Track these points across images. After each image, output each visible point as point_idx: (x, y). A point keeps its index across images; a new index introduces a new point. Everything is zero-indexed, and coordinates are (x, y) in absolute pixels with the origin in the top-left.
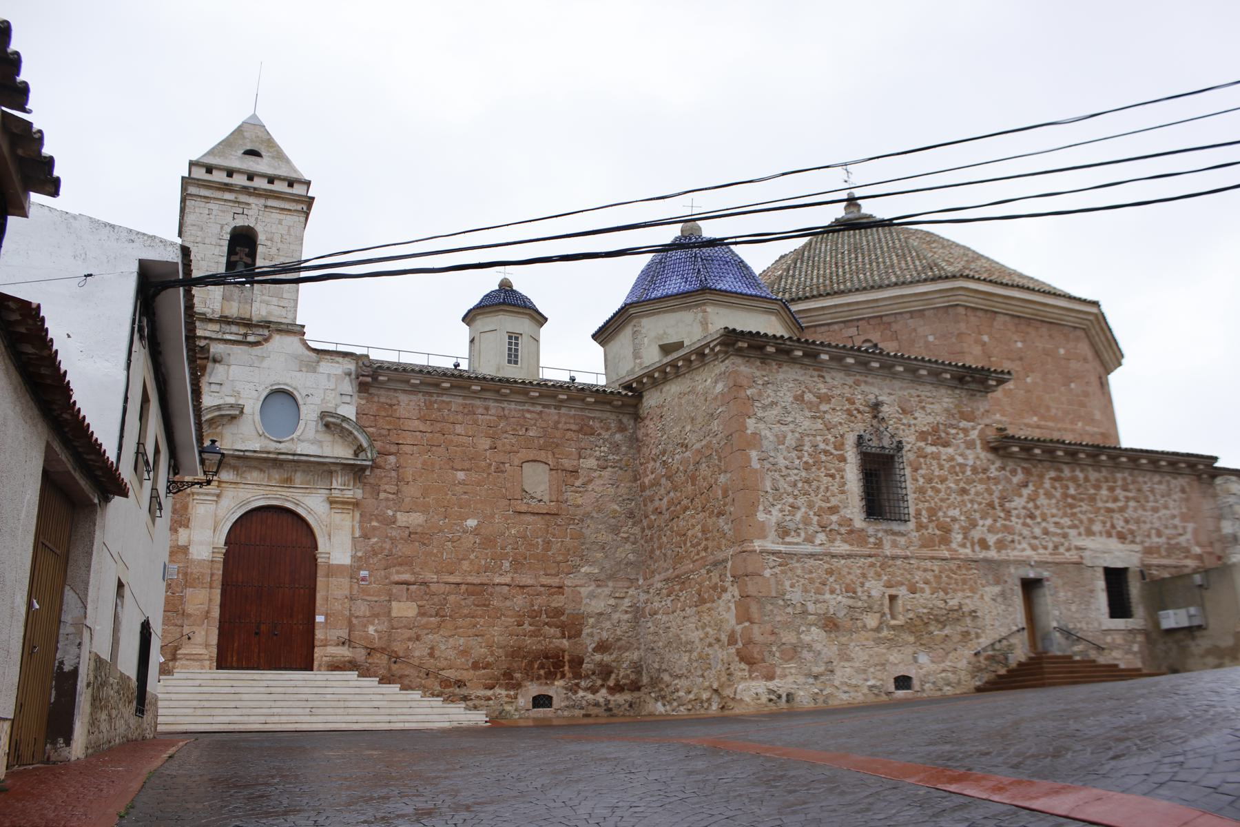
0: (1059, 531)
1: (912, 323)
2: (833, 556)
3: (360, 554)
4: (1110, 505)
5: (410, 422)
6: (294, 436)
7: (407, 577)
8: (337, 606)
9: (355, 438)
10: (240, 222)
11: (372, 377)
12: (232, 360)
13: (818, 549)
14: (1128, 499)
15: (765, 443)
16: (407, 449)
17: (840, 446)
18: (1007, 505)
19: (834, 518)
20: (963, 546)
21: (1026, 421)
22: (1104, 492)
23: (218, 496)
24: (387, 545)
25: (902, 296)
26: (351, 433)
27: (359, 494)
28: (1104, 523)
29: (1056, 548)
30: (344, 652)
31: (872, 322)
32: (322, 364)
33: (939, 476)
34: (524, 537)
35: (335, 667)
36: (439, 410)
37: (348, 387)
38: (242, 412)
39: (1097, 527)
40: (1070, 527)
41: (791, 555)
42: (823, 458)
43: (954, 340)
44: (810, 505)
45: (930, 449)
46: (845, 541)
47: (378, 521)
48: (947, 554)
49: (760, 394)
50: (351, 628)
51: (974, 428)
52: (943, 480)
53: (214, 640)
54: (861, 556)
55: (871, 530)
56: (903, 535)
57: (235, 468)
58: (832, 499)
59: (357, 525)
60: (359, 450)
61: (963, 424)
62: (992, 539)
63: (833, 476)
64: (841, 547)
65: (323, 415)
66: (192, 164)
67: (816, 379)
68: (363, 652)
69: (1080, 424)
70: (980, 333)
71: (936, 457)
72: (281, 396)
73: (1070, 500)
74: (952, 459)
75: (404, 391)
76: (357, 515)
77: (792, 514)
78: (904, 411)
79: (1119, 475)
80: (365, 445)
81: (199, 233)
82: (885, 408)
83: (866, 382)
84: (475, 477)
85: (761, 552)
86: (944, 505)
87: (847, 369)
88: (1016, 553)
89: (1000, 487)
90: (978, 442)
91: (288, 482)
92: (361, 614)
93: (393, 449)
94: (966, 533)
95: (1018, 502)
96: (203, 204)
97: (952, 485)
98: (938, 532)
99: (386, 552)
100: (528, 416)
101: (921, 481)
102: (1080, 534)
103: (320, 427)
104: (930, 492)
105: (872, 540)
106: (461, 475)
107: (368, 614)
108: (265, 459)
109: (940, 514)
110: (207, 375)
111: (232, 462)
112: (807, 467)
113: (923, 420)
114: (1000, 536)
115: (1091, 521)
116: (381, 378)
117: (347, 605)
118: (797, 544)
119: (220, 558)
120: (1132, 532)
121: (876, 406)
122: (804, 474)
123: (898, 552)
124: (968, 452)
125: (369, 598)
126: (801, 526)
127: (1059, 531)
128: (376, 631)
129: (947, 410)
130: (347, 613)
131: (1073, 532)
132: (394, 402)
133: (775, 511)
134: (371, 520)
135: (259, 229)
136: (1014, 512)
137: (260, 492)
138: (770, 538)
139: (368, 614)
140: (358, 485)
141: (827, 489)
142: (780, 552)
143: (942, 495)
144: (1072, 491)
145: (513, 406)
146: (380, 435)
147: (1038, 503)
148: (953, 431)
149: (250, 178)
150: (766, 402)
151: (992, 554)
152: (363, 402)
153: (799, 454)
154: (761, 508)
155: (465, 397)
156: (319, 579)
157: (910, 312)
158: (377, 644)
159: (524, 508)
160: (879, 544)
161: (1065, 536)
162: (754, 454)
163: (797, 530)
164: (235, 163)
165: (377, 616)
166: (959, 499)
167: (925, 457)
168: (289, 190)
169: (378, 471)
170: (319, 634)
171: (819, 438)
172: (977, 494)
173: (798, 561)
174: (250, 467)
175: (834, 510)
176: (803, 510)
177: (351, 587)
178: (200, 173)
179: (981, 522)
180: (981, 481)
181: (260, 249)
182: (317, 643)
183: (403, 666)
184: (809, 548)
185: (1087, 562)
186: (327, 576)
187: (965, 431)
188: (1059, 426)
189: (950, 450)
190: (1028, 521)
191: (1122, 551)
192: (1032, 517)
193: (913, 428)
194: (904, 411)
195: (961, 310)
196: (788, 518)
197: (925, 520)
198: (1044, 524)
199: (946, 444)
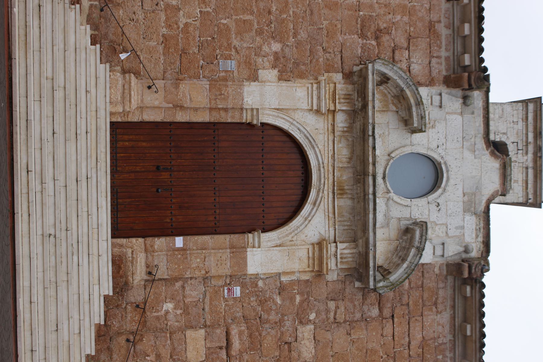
3: (260, 283)
5: (418, 328)
6: (392, 195)
7: (236, 345)
8: (195, 262)
9: (398, 266)
11: (467, 276)
12: (468, 117)
16: (388, 329)
23: (318, 112)
24: (273, 317)
26: (404, 260)
27: (332, 276)
30: (138, 274)
32: (474, 217)
35: (119, 265)
37: (453, 250)
38: (414, 131)
47: (302, 302)
50: (170, 281)
53: (149, 117)
57: (350, 129)
59: (294, 278)
60: (385, 272)
65: (423, 226)
68: (140, 299)
72: (436, 175)
75: (453, 318)
76: (306, 277)
80: (393, 278)
81: (497, 116)
91: (339, 191)
92: (188, 292)
93: (387, 312)
96: (521, 116)
99: (265, 316)
103: (404, 223)
107: (187, 300)
108: (364, 162)
110: (448, 90)
111: (358, 125)
116: (468, 288)
117: (197, 274)
119: (246, 118)
125: (207, 300)
128: (167, 312)
130: (188, 275)
132: (440, 307)
134: (301, 294)
137: (327, 160)
139: (187, 300)
140: (342, 274)
146: (401, 295)
152: (437, 270)
156: (228, 237)
158: (151, 315)
165: (186, 311)
169: (360, 296)
170: (159, 242)
174: (353, 146)
177: (220, 277)
182: (149, 240)
183: (123, 351)
186: (232, 247)
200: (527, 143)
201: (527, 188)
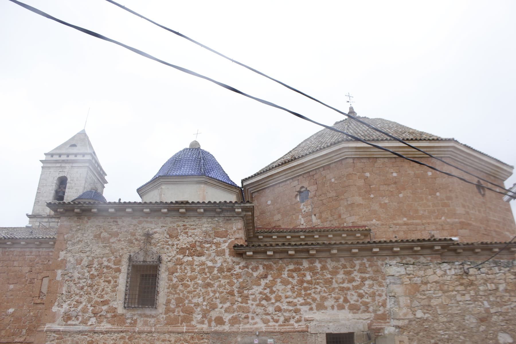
0: (291, 308)
1: (323, 173)
2: (95, 333)
4: (345, 285)
10: (61, 175)
13: (87, 328)
14: (363, 279)
15: (68, 265)
17: (118, 262)
18: (246, 292)
19: (105, 308)
20: (202, 323)
21: (395, 222)
22: (341, 276)
25: (315, 159)
28: (337, 299)
29: (287, 320)
31: (305, 176)
33: (190, 277)
34: (36, 317)
36: (8, 255)
39: (328, 303)
40: (301, 305)
41: (65, 332)
42: (105, 270)
43: (345, 179)
44: (89, 301)
45: (186, 259)
46: (109, 322)
48: (185, 329)
49: (73, 237)
51: (225, 242)
52: (192, 279)
54: (115, 332)
55: (128, 315)
56: (153, 317)
58: (105, 296)
61: (217, 240)
62: (227, 317)
63: (109, 282)
64: (105, 326)
66: (46, 154)
67: (112, 224)
69: (443, 218)
70: (364, 172)
71: (191, 264)
73: (305, 285)
74: (203, 264)
77: (76, 306)
78: (171, 236)
79: (357, 262)
82: (156, 236)
83: (146, 221)
84: (18, 286)
85: (46, 331)
86: (190, 295)
87: (130, 215)
88: (248, 326)
89: (241, 280)
90: (227, 252)
94: (205, 314)
95: (257, 290)
97: (200, 282)
98: (181, 314)
100: (51, 254)
101: (175, 280)
102: (311, 309)
104: (180, 287)
105: (129, 321)
106: (12, 287)
109: (187, 301)
112: (92, 277)
113: (184, 241)
114: (236, 314)
115: (324, 299)
118: (75, 325)
120: (366, 304)
121: (148, 236)
122: (89, 282)
123: (147, 328)
124: (217, 258)
126: (80, 314)
127: (291, 308)
129: (206, 233)
131: (304, 309)
133: (65, 306)
135: (68, 177)
136: (251, 297)
138: (57, 322)
141: (103, 290)
142: (59, 331)
143: (191, 288)
144: (308, 278)
145: (44, 250)
147: (274, 289)
148: (208, 245)
149: (68, 156)
150: (76, 241)
151: (226, 328)
153: (89, 269)
154: (56, 304)
155: (21, 248)
157: (323, 167)
159: (39, 301)
160: (134, 323)
161: (297, 311)
162: (59, 272)
163: (76, 317)
164: (63, 151)
166: (203, 290)
167: (182, 264)
168: (83, 158)
171: (104, 259)
172: (220, 286)
173: (70, 336)
175: (105, 303)
176: (84, 304)
178: (49, 158)
179: (220, 306)
180: (225, 277)
181: (68, 185)
184: (81, 328)
185: (311, 330)
187: (218, 244)
188: (424, 221)
189: (203, 258)
190: (264, 302)
191: (348, 320)
192: (267, 299)
193: (175, 247)
194: (171, 236)
195: (351, 161)
196: (72, 309)
197: (172, 306)
198: (278, 304)
199: (200, 255)
200: (61, 167)
201: (81, 167)
